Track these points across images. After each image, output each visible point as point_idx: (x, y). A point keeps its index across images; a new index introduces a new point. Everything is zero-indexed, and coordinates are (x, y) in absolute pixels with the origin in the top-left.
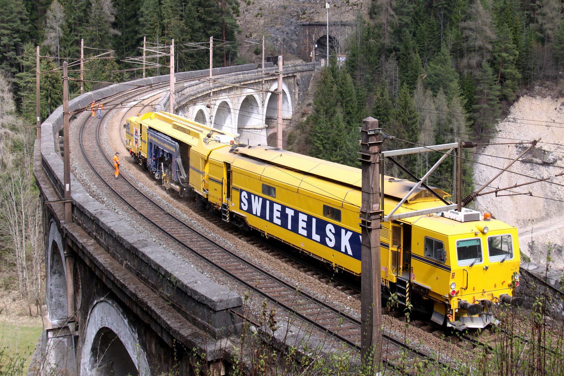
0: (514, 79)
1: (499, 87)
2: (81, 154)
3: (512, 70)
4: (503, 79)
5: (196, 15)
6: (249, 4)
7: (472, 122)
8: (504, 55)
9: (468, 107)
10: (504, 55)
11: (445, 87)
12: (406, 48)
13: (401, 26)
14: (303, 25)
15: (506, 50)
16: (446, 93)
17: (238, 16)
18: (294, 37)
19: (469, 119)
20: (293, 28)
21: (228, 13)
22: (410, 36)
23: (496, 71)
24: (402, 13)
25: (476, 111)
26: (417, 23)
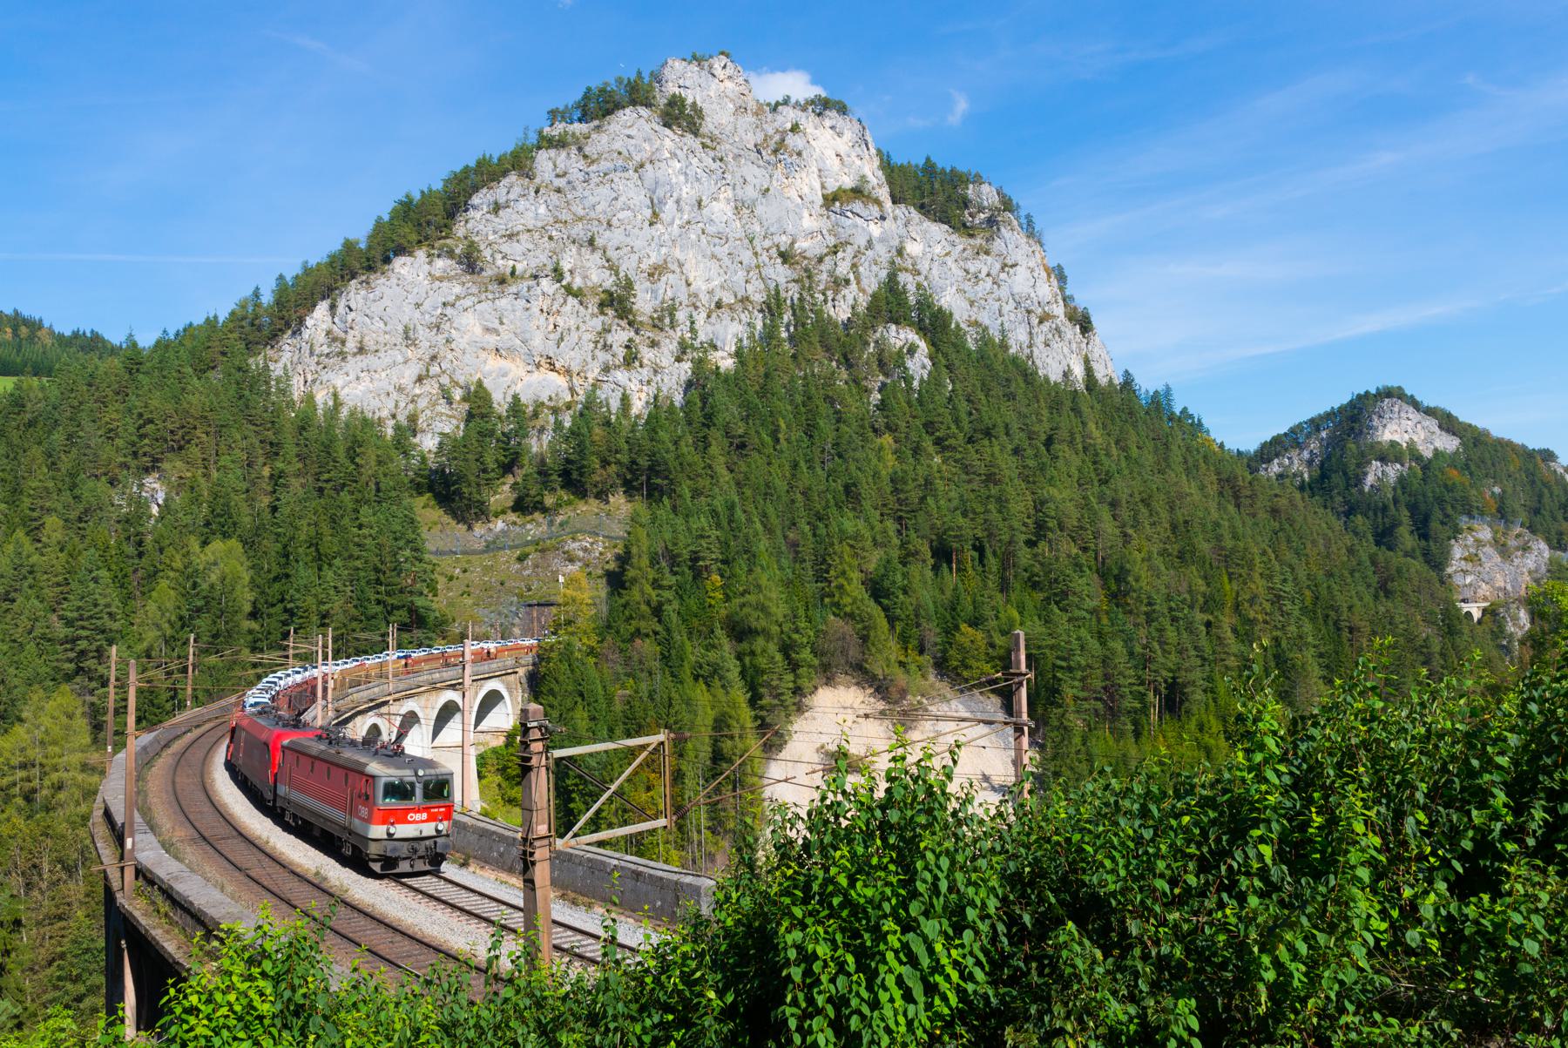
0: (810, 666)
1: (790, 677)
2: (172, 798)
3: (806, 654)
4: (794, 666)
5: (373, 597)
6: (451, 578)
7: (759, 722)
8: (796, 636)
9: (753, 702)
10: (796, 636)
11: (721, 678)
12: (668, 630)
13: (660, 604)
14: (530, 605)
15: (797, 631)
16: (723, 686)
17: (436, 595)
18: (517, 621)
19: (756, 718)
20: (514, 609)
21: (421, 594)
22: (674, 617)
23: (787, 657)
24: (660, 587)
25: (762, 708)
26: (681, 598)
